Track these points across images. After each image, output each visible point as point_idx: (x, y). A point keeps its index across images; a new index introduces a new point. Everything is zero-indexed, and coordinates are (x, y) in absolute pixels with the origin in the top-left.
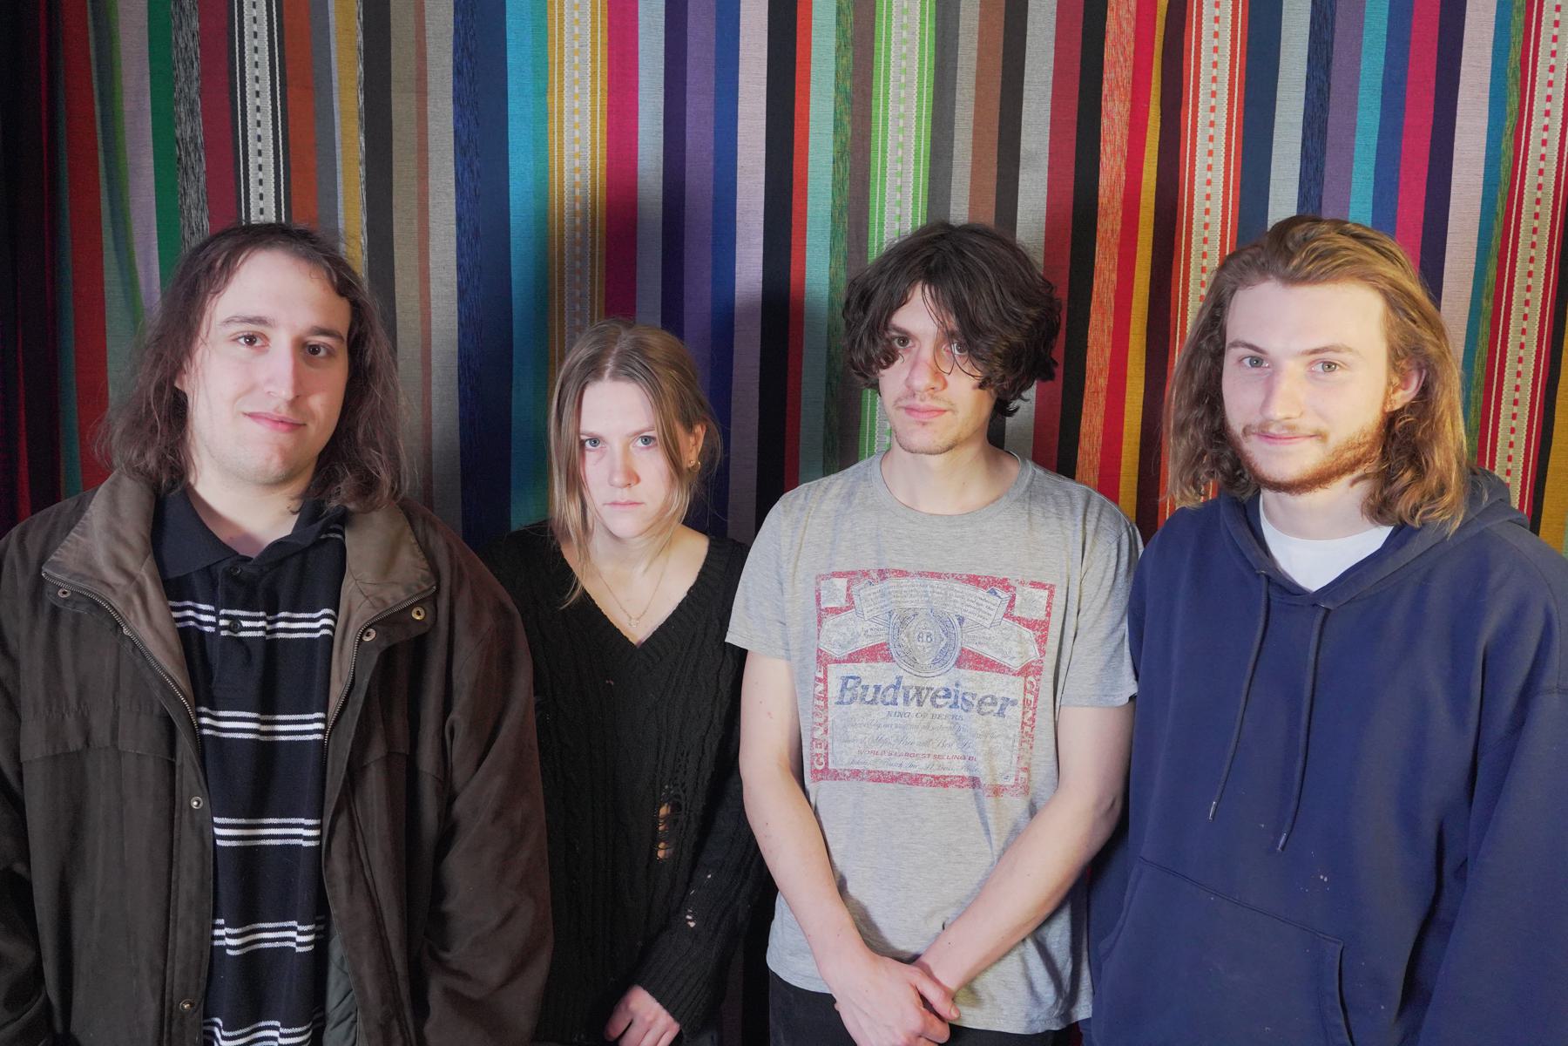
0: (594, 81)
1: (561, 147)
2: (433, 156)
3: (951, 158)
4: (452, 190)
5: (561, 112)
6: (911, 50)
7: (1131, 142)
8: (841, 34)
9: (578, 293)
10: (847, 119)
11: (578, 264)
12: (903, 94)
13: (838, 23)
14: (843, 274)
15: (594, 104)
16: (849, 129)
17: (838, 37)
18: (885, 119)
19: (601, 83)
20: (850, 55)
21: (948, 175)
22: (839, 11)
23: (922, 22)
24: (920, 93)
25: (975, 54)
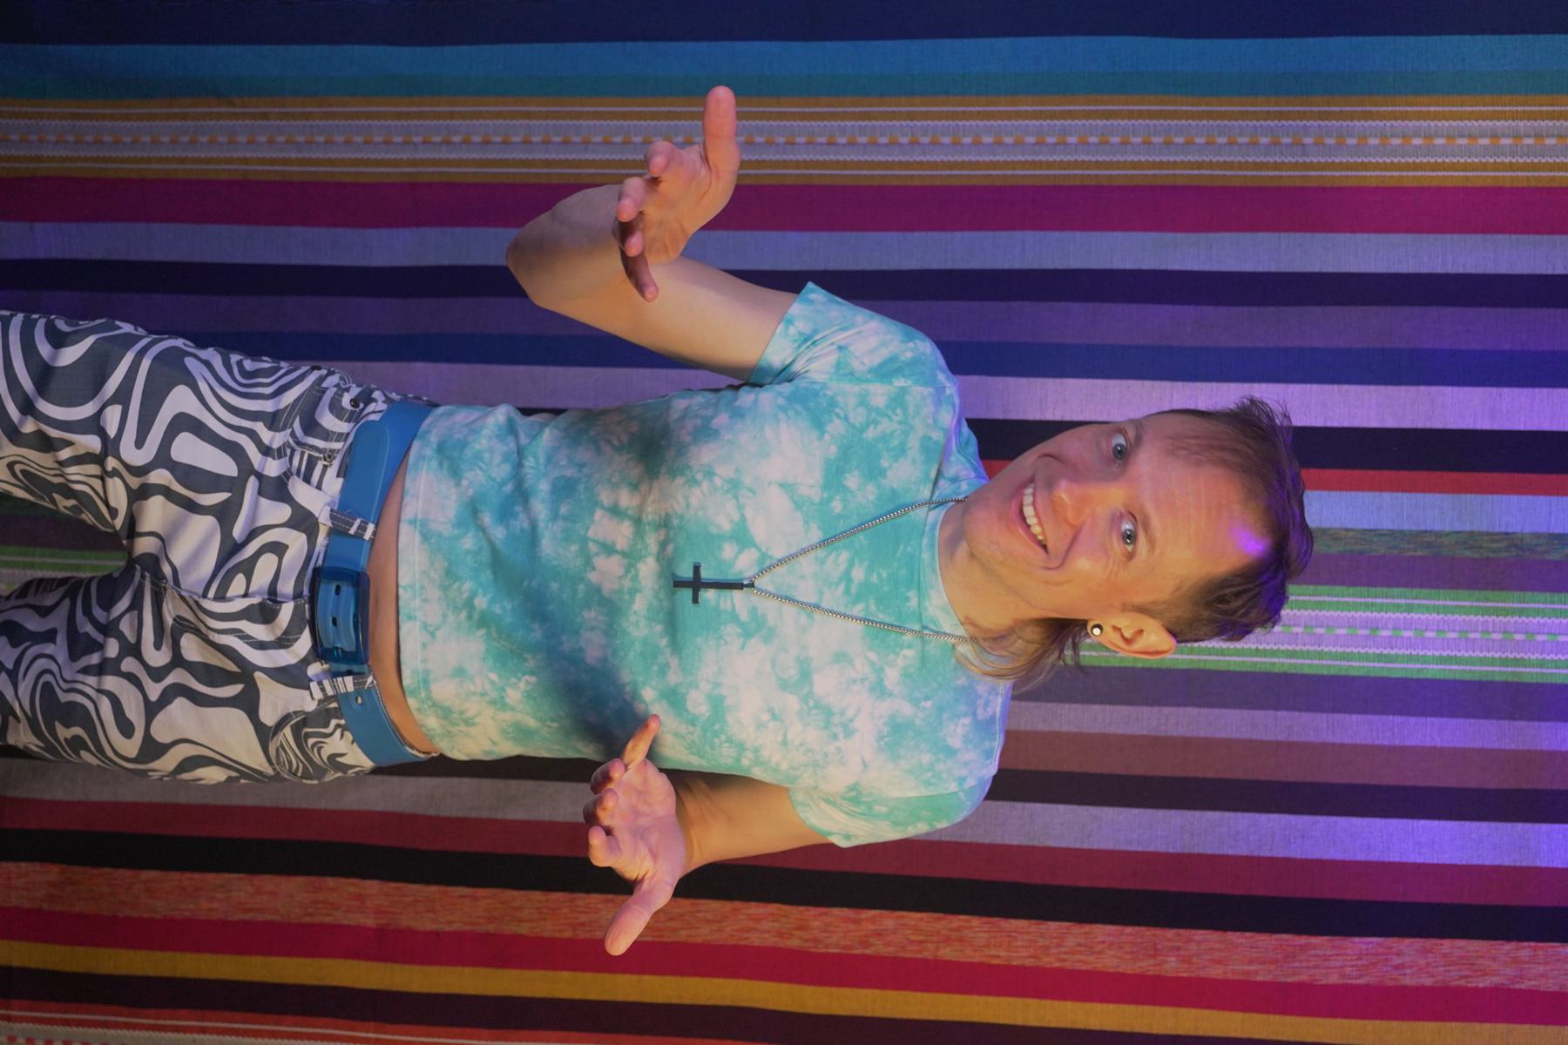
3: (1512, 718)
7: (1533, 995)
9: (1308, 140)
11: (1351, 141)
14: (1335, 549)
16: (1555, 556)
21: (1488, 713)
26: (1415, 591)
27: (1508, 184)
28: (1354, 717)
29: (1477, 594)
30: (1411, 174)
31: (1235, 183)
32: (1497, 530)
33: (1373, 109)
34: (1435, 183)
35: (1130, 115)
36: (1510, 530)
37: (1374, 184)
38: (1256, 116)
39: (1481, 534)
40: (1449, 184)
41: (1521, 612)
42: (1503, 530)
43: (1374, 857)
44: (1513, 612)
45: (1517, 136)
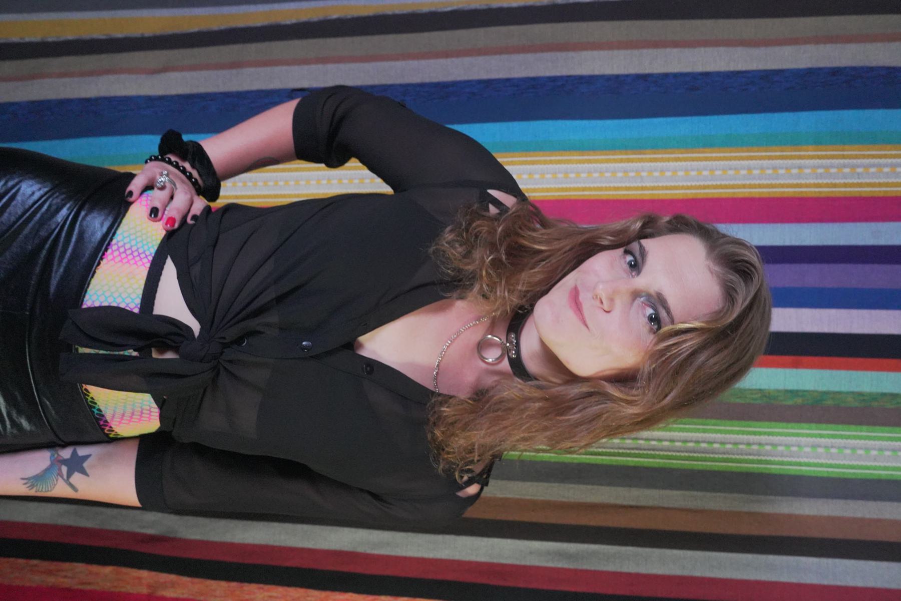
0: (827, 185)
1: (770, 158)
2: (761, 51)
4: (732, 67)
5: (800, 157)
6: (860, 457)
8: (874, 397)
9: (644, 174)
10: (799, 401)
11: (668, 174)
12: (820, 450)
13: (884, 395)
15: (807, 186)
16: (790, 403)
17: (870, 394)
18: (798, 435)
19: (825, 191)
20: (856, 404)
22: (894, 396)
23: (886, 468)
24: (822, 465)
25: (859, 515)
26: (709, 421)
27: (757, 196)
28: (675, 493)
29: (743, 423)
30: (702, 191)
31: (604, 198)
32: (754, 387)
33: (680, 156)
34: (716, 196)
35: (545, 162)
36: (763, 387)
37: (681, 197)
38: (615, 161)
39: (745, 390)
40: (724, 196)
41: (769, 434)
42: (758, 387)
43: (686, 573)
44: (765, 433)
45: (762, 169)
